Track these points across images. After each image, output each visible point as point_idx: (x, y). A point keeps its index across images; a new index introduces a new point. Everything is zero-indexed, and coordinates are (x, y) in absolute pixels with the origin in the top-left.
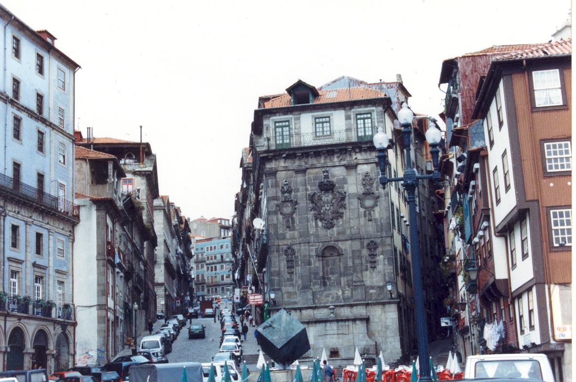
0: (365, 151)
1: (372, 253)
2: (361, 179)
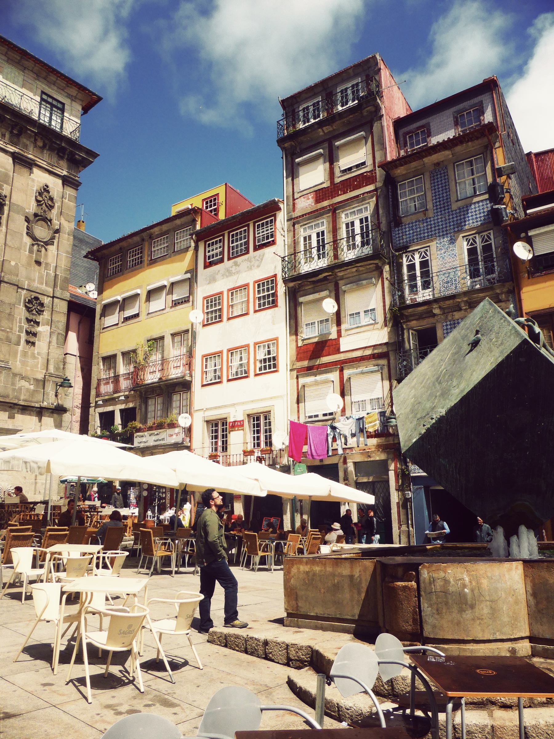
0: (51, 149)
1: (34, 317)
2: (35, 189)
